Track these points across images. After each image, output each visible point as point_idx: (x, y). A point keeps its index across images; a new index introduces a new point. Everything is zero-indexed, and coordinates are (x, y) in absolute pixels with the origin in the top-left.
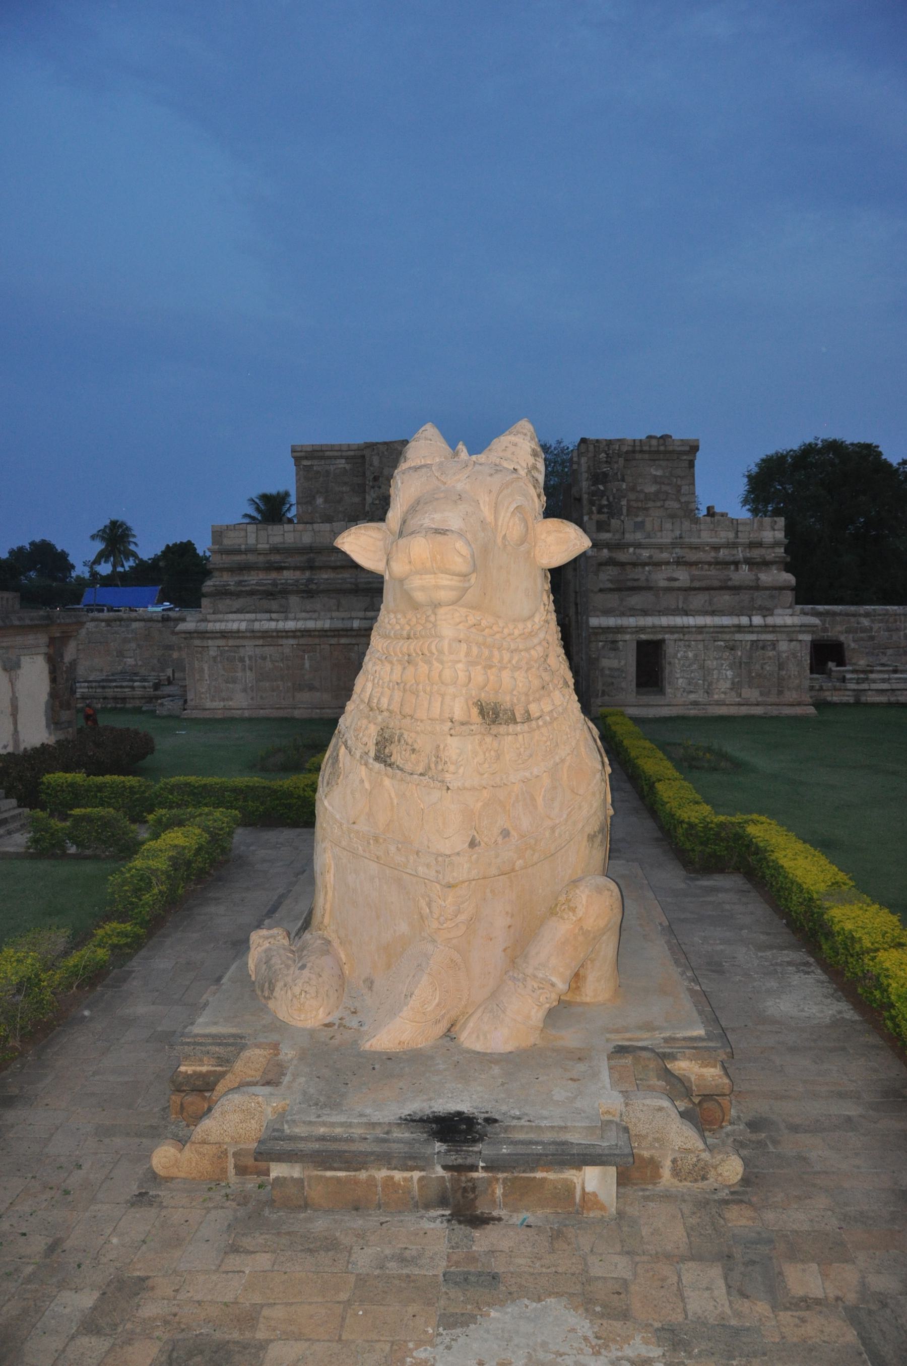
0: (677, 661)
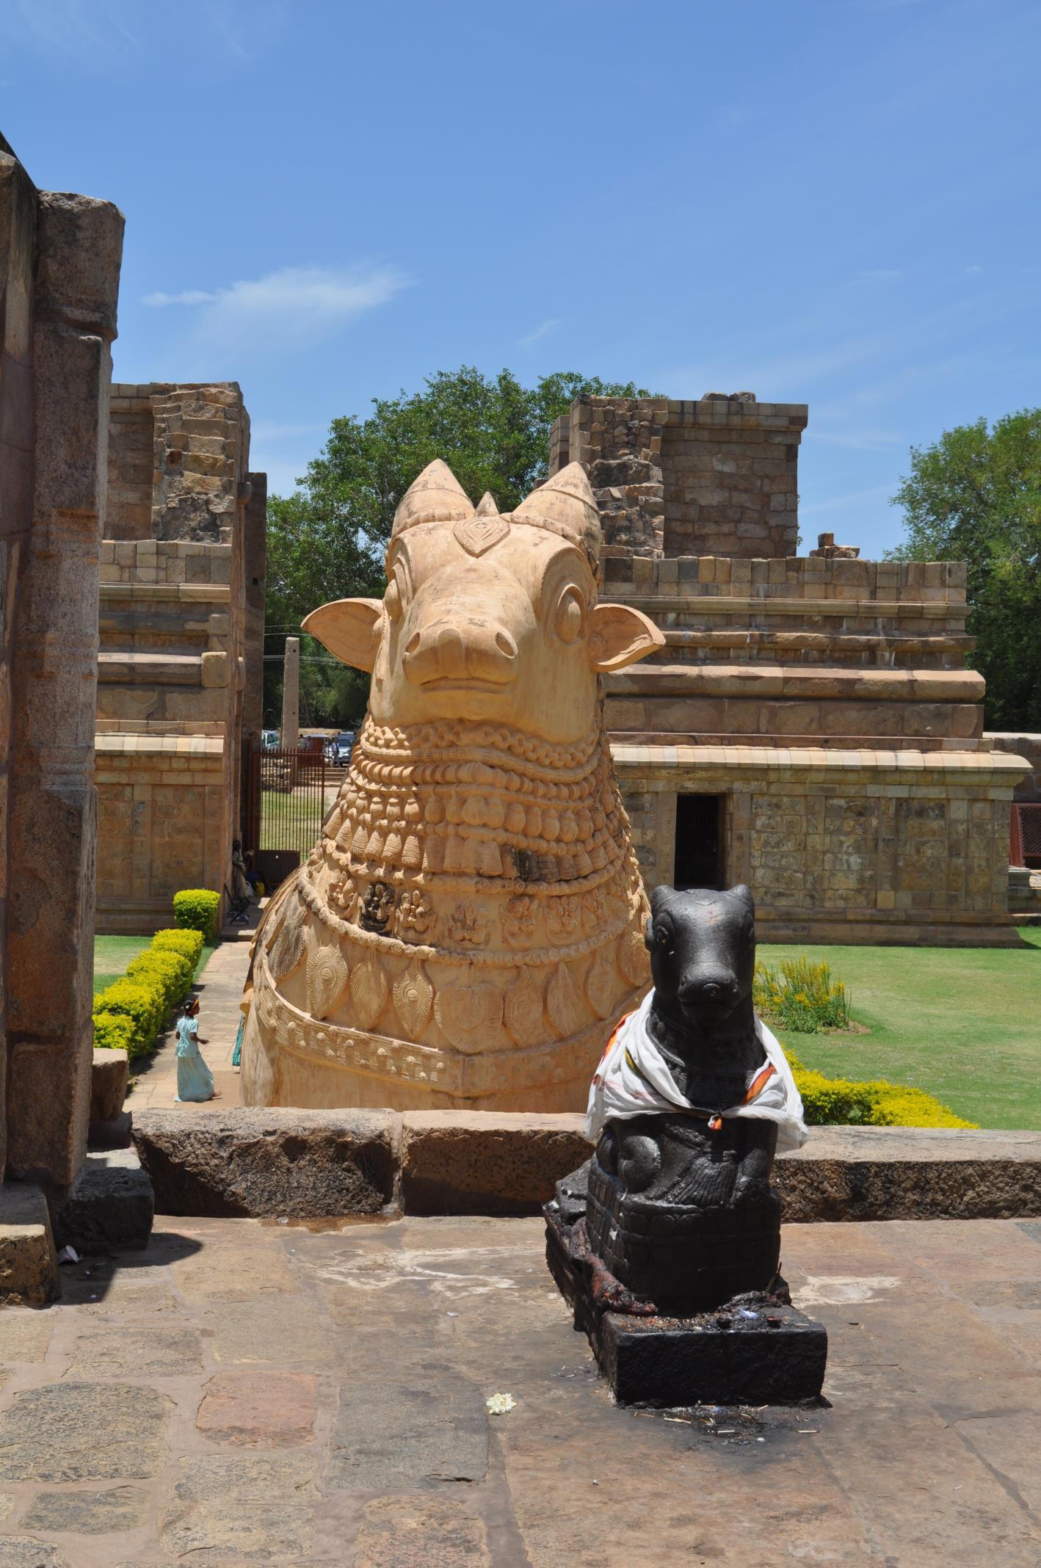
0: (754, 835)
